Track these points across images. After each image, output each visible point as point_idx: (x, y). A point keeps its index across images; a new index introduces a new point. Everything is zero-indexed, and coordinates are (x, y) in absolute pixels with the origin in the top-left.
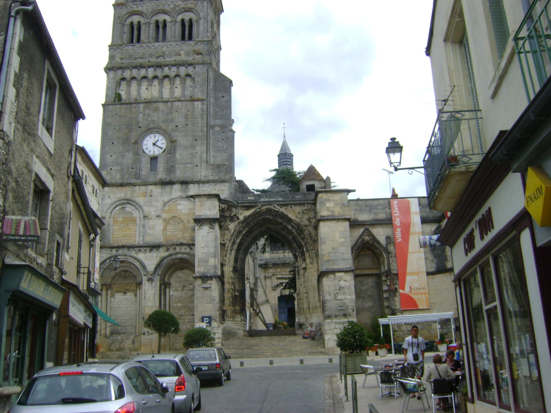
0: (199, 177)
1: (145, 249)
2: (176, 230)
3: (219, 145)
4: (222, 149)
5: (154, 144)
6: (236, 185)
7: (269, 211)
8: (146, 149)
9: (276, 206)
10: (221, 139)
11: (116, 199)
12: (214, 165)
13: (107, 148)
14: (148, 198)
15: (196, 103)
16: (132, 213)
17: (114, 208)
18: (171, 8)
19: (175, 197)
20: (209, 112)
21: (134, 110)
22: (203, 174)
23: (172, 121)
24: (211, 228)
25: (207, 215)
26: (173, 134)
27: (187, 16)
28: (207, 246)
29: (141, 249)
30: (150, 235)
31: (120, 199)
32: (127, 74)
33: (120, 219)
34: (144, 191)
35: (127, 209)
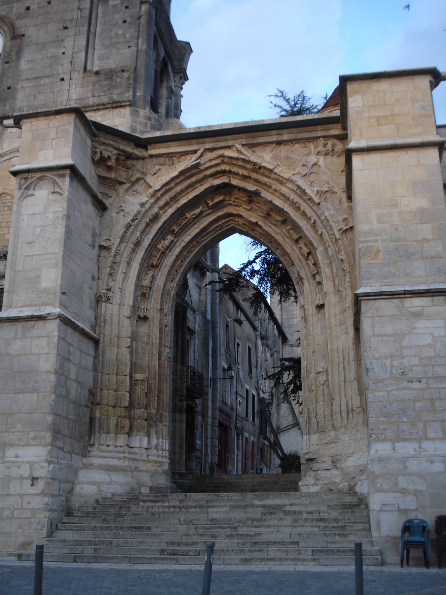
0: (64, 103)
3: (116, 34)
4: (121, 40)
10: (121, 22)
22: (74, 96)
26: (18, 23)
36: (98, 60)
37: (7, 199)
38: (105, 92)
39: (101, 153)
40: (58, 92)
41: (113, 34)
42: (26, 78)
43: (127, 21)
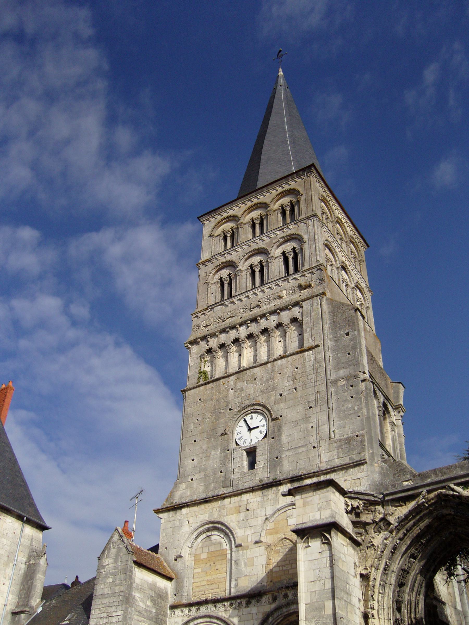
1: (239, 601)
2: (287, 562)
4: (352, 412)
5: (250, 429)
6: (382, 468)
7: (445, 501)
8: (239, 439)
9: (456, 488)
11: (198, 525)
12: (340, 440)
13: (187, 449)
14: (242, 515)
15: (306, 354)
16: (220, 543)
17: (196, 539)
18: (266, 244)
19: (284, 504)
20: (327, 362)
21: (222, 387)
23: (274, 388)
24: (324, 543)
25: (315, 520)
26: (276, 408)
27: (288, 246)
28: (320, 579)
29: (234, 602)
30: (246, 575)
31: (202, 522)
32: (214, 343)
33: (204, 556)
34: (237, 505)
35: (213, 537)
36: (338, 429)
37: (287, 543)
38: (346, 454)
39: (352, 505)
40: (312, 457)
41: (345, 408)
42: (288, 449)
43: (354, 397)
